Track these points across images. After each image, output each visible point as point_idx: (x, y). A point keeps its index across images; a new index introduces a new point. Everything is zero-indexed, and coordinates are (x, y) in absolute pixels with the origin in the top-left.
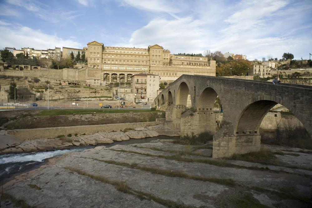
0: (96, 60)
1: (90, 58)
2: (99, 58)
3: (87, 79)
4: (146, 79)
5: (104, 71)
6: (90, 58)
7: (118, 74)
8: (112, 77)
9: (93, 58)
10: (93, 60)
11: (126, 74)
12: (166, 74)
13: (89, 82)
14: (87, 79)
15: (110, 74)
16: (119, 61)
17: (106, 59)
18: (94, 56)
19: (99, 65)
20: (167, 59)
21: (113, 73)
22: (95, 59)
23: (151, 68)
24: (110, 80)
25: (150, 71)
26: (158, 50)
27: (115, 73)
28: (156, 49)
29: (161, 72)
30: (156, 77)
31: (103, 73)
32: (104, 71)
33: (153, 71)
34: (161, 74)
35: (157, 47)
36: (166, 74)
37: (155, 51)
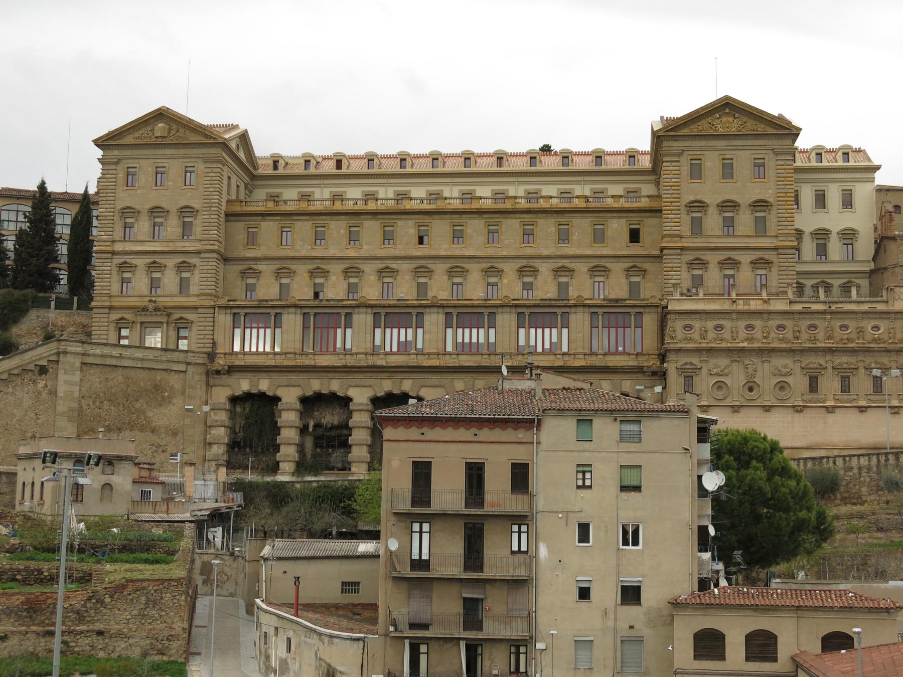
0: (170, 280)
1: (118, 260)
2: (193, 260)
3: (21, 458)
4: (519, 454)
5: (232, 370)
6: (118, 260)
7: (360, 396)
8: (303, 430)
9: (141, 262)
10: (140, 283)
11: (360, 396)
12: (830, 384)
13: (29, 481)
14: (21, 458)
15: (290, 396)
16: (373, 278)
17: (261, 267)
18: (153, 238)
19: (190, 316)
20: (849, 236)
21: (316, 385)
22: (154, 266)
23: (676, 326)
24: (288, 454)
25: (663, 357)
26: (743, 159)
27: (335, 385)
28: (722, 143)
29: (780, 362)
30: (652, 429)
31: (221, 395)
32: (232, 370)
33: (695, 360)
34: (782, 386)
35: (727, 123)
36: (830, 384)
37: (711, 162)
